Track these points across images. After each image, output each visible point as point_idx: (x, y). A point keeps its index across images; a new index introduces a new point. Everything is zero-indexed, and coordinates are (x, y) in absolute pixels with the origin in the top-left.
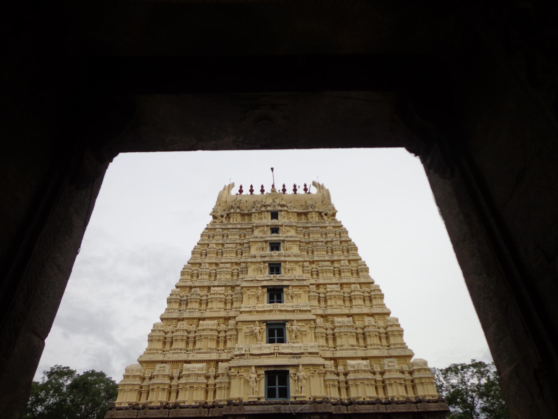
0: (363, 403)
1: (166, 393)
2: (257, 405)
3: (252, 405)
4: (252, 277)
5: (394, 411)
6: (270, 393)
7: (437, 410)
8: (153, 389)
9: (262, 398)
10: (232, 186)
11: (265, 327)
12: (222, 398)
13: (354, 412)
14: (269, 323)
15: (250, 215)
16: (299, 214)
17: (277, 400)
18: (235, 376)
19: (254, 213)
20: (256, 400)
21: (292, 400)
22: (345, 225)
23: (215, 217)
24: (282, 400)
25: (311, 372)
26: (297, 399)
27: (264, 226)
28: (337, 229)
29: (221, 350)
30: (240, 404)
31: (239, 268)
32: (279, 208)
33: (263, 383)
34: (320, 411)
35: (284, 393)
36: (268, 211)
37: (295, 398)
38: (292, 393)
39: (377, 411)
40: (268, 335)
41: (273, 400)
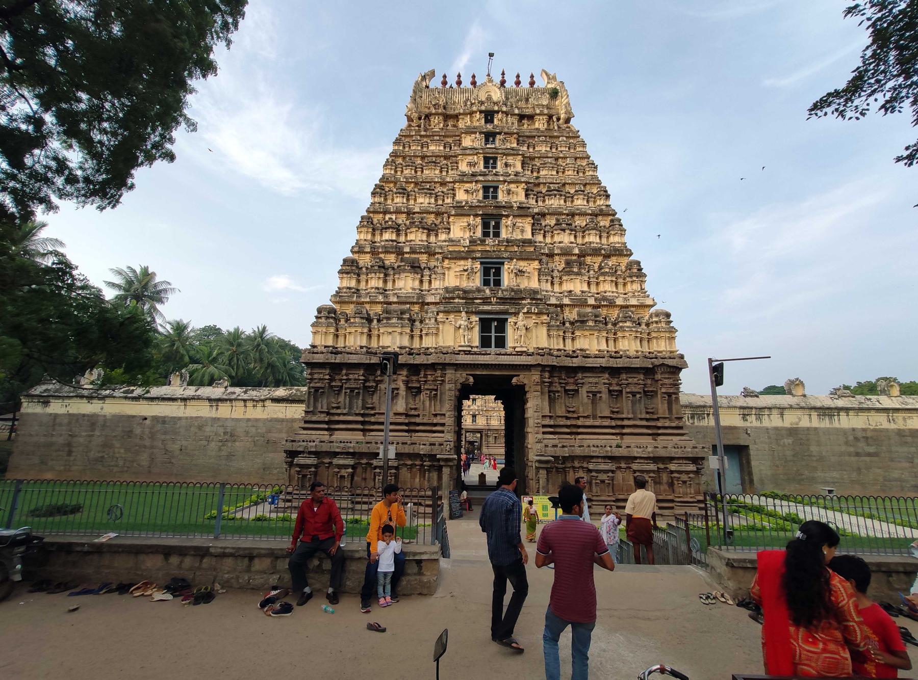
1: (365, 337)
4: (461, 202)
6: (485, 342)
8: (350, 333)
10: (432, 74)
11: (479, 266)
12: (430, 346)
15: (456, 117)
16: (522, 117)
18: (444, 322)
20: (469, 349)
21: (509, 350)
22: (583, 135)
23: (410, 119)
25: (534, 321)
26: (517, 349)
27: (475, 133)
28: (572, 141)
29: (426, 290)
31: (445, 190)
32: (496, 108)
33: (477, 329)
35: (501, 342)
37: (515, 348)
38: (510, 343)
41: (488, 350)
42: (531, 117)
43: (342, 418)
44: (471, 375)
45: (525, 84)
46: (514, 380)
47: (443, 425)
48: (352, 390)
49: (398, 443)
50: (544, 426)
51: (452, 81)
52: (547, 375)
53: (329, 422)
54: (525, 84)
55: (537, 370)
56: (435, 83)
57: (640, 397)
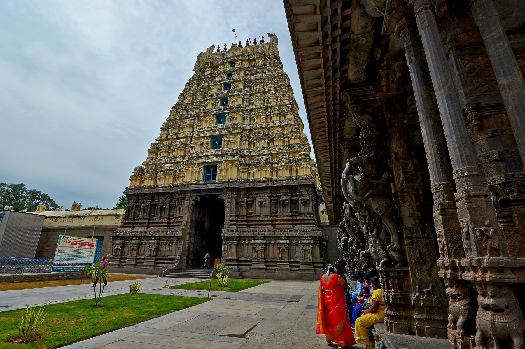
0: (260, 182)
2: (198, 185)
3: (194, 185)
5: (278, 185)
7: (306, 183)
9: (201, 181)
13: (253, 187)
14: (212, 137)
15: (217, 67)
17: (211, 181)
19: (220, 65)
24: (214, 181)
30: (188, 184)
34: (231, 187)
35: (214, 177)
36: (228, 62)
39: (267, 186)
40: (212, 144)
41: (208, 182)
42: (255, 60)
43: (139, 221)
44: (198, 195)
45: (258, 42)
46: (219, 197)
47: (182, 222)
48: (144, 206)
49: (159, 232)
50: (231, 221)
51: (222, 49)
52: (234, 193)
53: (134, 223)
54: (258, 42)
55: (229, 191)
56: (215, 51)
57: (288, 203)
